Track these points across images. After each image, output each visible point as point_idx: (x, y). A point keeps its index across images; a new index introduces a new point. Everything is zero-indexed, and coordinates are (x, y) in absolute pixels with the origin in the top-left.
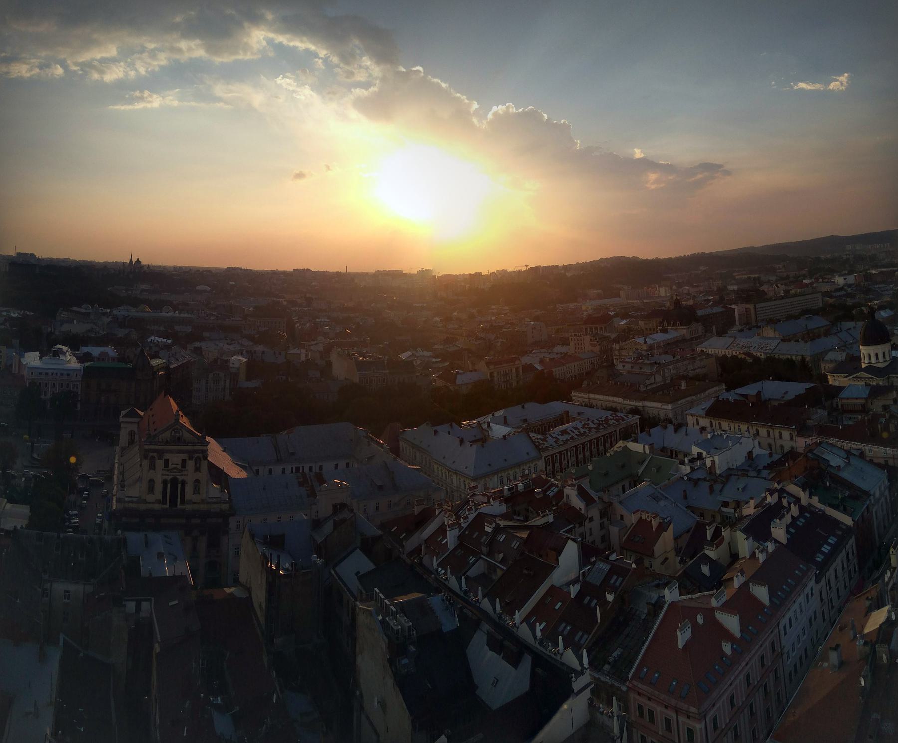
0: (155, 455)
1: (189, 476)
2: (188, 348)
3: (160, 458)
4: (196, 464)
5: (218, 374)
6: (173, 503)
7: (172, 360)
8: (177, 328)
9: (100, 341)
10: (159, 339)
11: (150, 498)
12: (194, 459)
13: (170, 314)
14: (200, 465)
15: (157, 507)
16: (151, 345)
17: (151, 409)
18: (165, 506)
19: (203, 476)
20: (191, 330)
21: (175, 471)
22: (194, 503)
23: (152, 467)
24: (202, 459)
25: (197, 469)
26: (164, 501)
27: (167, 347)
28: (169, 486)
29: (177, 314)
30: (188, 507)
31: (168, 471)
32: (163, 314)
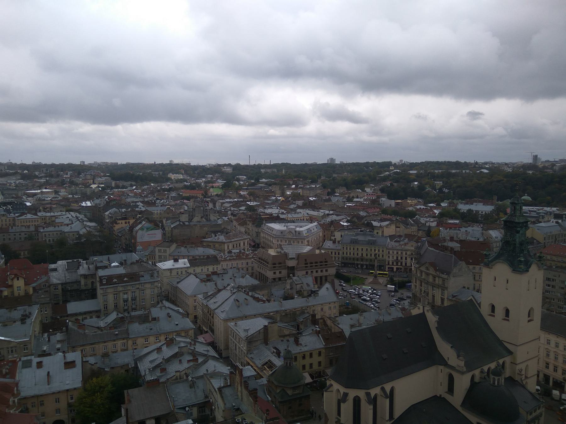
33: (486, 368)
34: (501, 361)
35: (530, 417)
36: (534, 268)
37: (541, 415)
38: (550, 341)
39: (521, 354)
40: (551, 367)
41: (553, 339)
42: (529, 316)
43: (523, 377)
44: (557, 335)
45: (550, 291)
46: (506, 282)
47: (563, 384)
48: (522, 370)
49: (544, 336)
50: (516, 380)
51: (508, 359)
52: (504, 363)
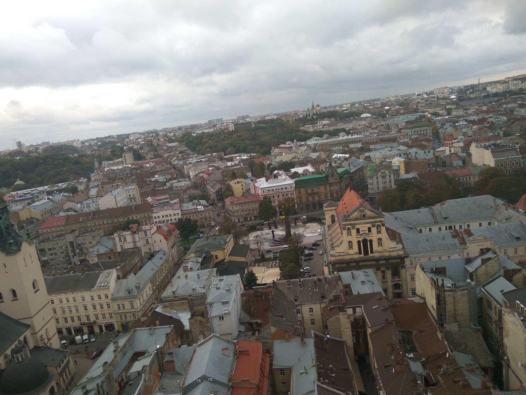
0: (350, 226)
1: (374, 236)
2: (361, 158)
3: (353, 228)
4: (377, 229)
5: (385, 172)
6: (366, 253)
7: (352, 167)
8: (352, 146)
9: (302, 164)
10: (341, 155)
11: (351, 252)
12: (376, 226)
13: (346, 137)
14: (380, 230)
15: (357, 256)
16: (336, 160)
17: (343, 200)
18: (361, 256)
19: (384, 235)
20: (361, 145)
21: (364, 235)
22: (379, 252)
23: (349, 234)
24: (381, 226)
25: (379, 232)
26: (360, 253)
27: (346, 159)
28: (362, 244)
29: (350, 137)
30: (376, 255)
31: (360, 235)
32: (341, 138)
33: (8, 352)
34: (22, 338)
35: (59, 370)
36: (25, 246)
37: (68, 362)
38: (61, 300)
39: (37, 323)
40: (69, 320)
41: (63, 296)
42: (34, 288)
43: (46, 341)
44: (65, 292)
45: (54, 259)
46: (4, 266)
47: (81, 328)
48: (42, 335)
49: (55, 298)
50: (41, 346)
51: (28, 333)
52: (25, 338)
